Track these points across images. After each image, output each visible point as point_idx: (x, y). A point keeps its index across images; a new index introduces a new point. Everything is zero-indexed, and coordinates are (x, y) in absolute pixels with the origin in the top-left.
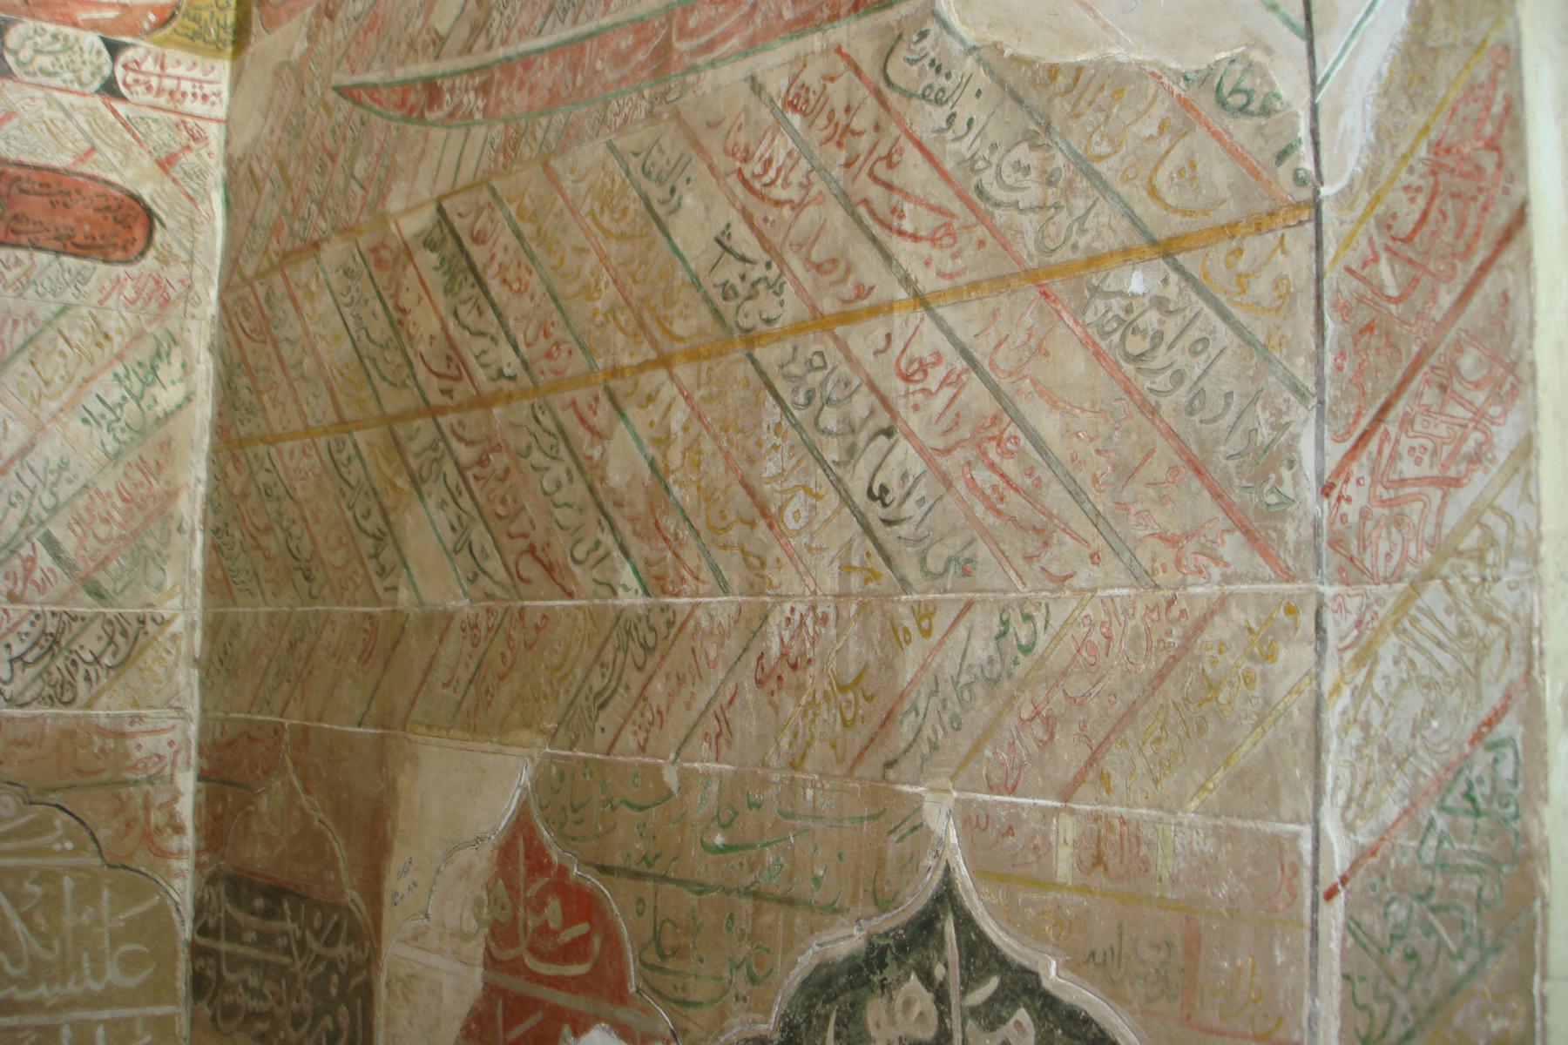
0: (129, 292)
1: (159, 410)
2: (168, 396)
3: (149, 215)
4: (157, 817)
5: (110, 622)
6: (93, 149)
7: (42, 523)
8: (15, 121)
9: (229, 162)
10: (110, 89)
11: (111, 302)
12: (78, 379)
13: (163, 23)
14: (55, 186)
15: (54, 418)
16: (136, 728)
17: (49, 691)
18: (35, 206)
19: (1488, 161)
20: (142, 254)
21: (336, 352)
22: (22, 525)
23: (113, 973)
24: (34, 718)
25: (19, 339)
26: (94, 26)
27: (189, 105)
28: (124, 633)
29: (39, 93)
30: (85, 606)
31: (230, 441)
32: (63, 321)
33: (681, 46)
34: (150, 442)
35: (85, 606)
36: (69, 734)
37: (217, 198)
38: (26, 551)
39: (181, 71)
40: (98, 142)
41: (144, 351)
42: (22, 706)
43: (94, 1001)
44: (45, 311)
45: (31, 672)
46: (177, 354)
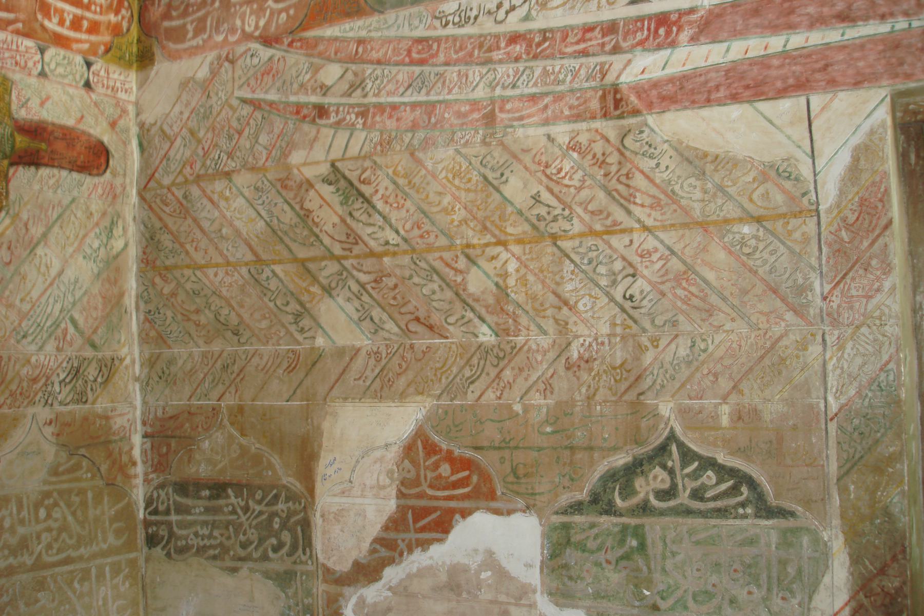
0: (100, 191)
1: (115, 252)
2: (118, 244)
3: (107, 153)
5: (100, 360)
6: (82, 117)
7: (69, 311)
8: (50, 101)
9: (142, 125)
10: (88, 85)
11: (93, 196)
12: (80, 236)
13: (107, 51)
14: (69, 135)
15: (71, 256)
16: (113, 414)
17: (76, 397)
18: (60, 146)
19: (880, 205)
20: (105, 171)
22: (61, 312)
23: (111, 539)
24: (70, 412)
25: (55, 216)
26: (79, 52)
28: (106, 366)
29: (60, 87)
30: (89, 353)
32: (73, 206)
33: (501, 116)
34: (111, 269)
35: (89, 353)
36: (86, 419)
37: (134, 143)
38: (63, 325)
39: (116, 76)
40: (85, 113)
41: (106, 222)
42: (66, 405)
43: (103, 554)
44: (65, 202)
45: (69, 387)
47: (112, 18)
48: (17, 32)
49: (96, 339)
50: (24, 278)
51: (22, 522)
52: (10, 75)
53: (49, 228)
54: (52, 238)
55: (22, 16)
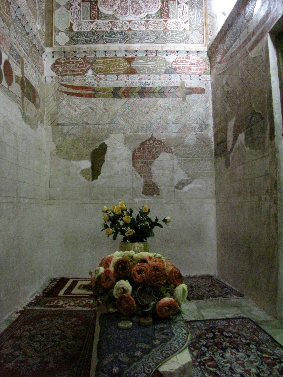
2: (208, 105)
4: (210, 141)
10: (200, 79)
14: (196, 88)
18: (195, 90)
21: (220, 96)
23: (208, 155)
26: (198, 74)
27: (207, 80)
31: (214, 108)
35: (203, 123)
41: (206, 101)
43: (207, 157)
46: (208, 102)
47: (204, 67)
48: (186, 74)
49: (204, 121)
50: (190, 112)
51: (190, 150)
52: (184, 81)
53: (194, 104)
54: (195, 105)
55: (186, 71)
